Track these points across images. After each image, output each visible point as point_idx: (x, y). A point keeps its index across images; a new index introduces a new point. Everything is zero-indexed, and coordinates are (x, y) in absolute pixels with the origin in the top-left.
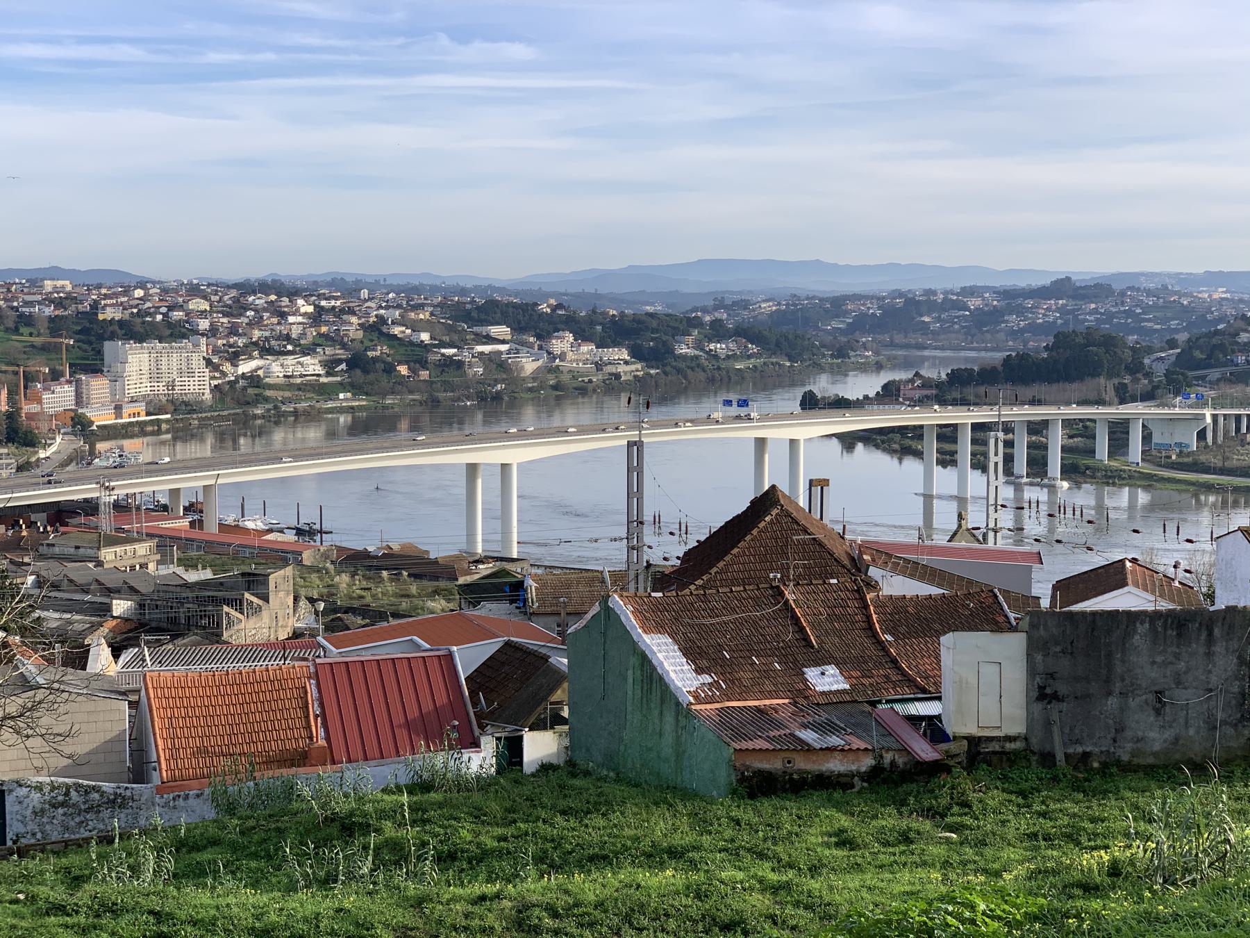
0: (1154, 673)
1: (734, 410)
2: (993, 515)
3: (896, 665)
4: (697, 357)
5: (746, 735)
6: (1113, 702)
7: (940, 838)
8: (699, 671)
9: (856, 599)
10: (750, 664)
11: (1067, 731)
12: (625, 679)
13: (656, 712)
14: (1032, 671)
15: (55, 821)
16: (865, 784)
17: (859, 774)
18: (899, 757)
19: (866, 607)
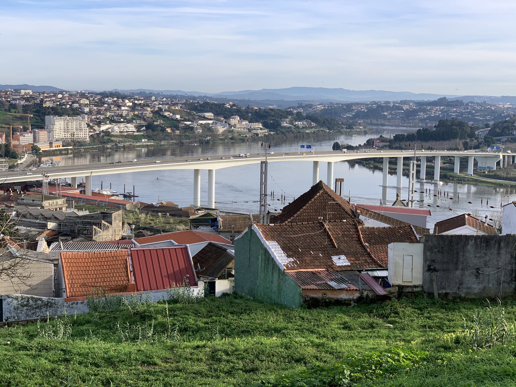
0: (476, 261)
1: (305, 150)
2: (411, 195)
3: (369, 255)
4: (290, 127)
5: (307, 283)
6: (458, 273)
7: (386, 326)
8: (289, 256)
9: (354, 228)
10: (309, 254)
11: (439, 284)
12: (258, 259)
13: (270, 273)
14: (425, 259)
15: (23, 312)
16: (356, 304)
17: (353, 300)
18: (370, 293)
19: (358, 232)
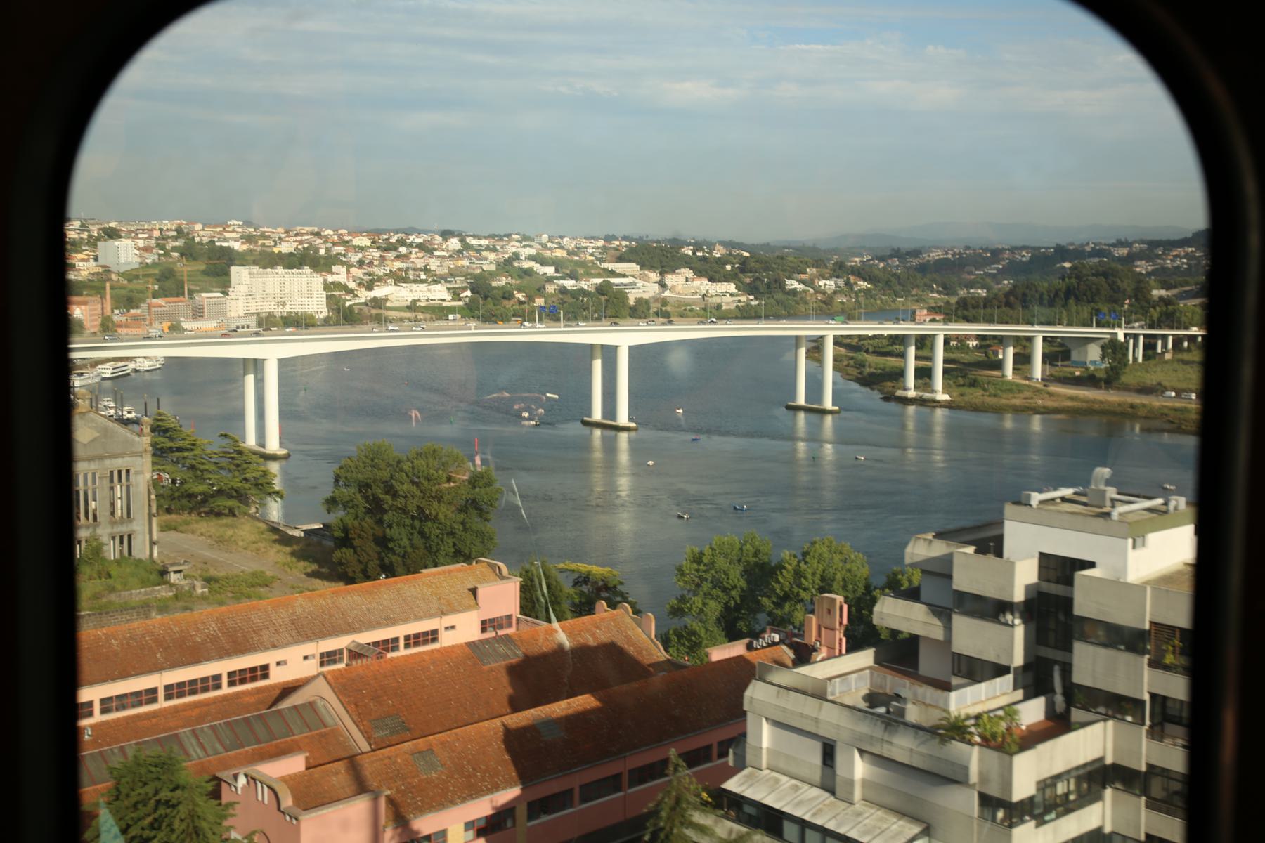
4: (804, 291)
